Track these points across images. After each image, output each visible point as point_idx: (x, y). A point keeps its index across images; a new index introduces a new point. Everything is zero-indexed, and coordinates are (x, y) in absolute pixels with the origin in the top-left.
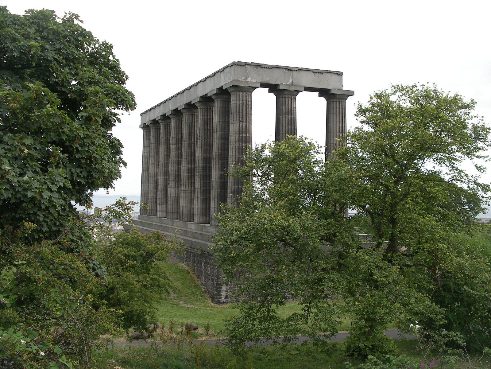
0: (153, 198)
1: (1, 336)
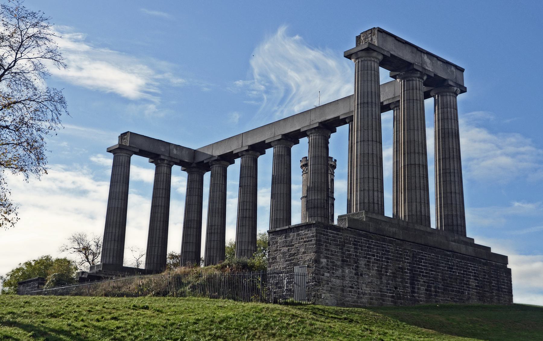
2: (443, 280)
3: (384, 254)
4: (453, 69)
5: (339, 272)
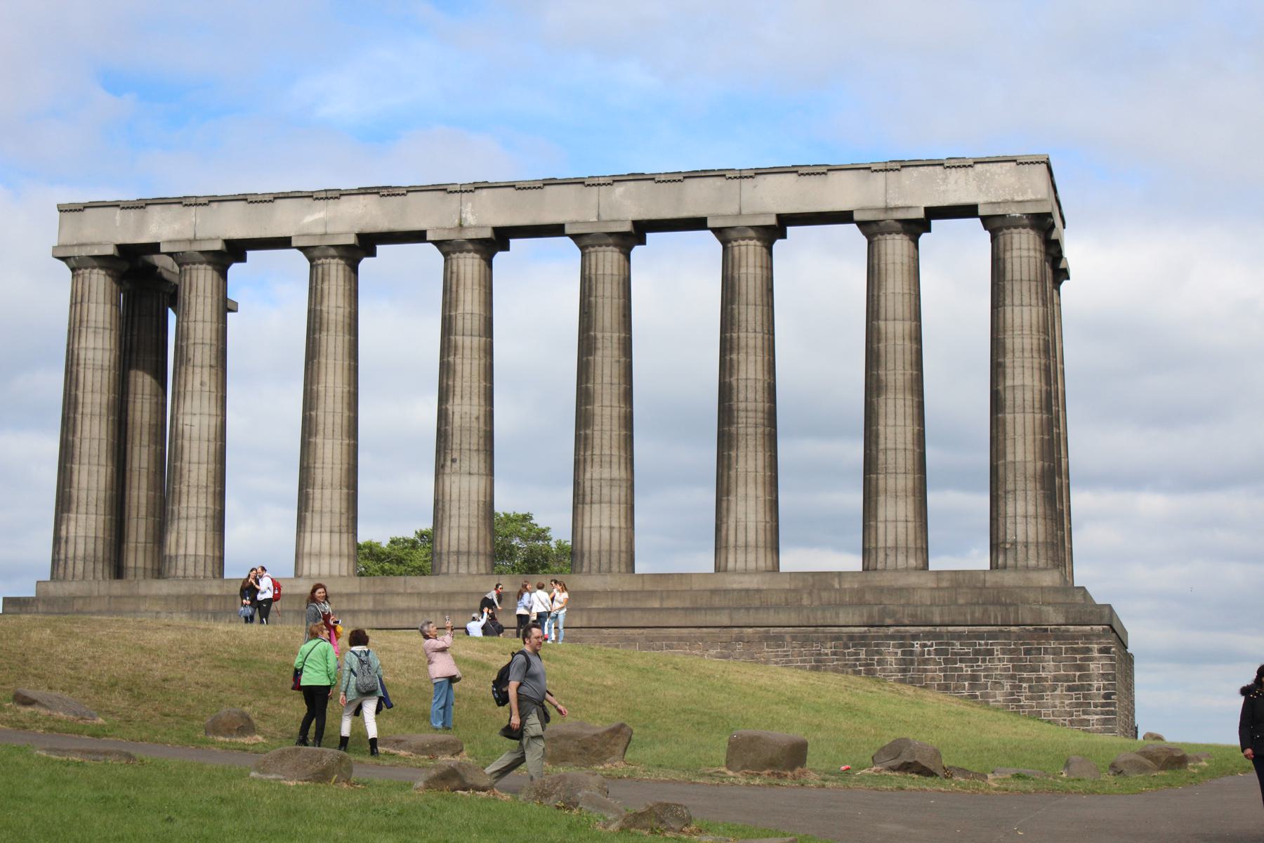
0: (210, 512)
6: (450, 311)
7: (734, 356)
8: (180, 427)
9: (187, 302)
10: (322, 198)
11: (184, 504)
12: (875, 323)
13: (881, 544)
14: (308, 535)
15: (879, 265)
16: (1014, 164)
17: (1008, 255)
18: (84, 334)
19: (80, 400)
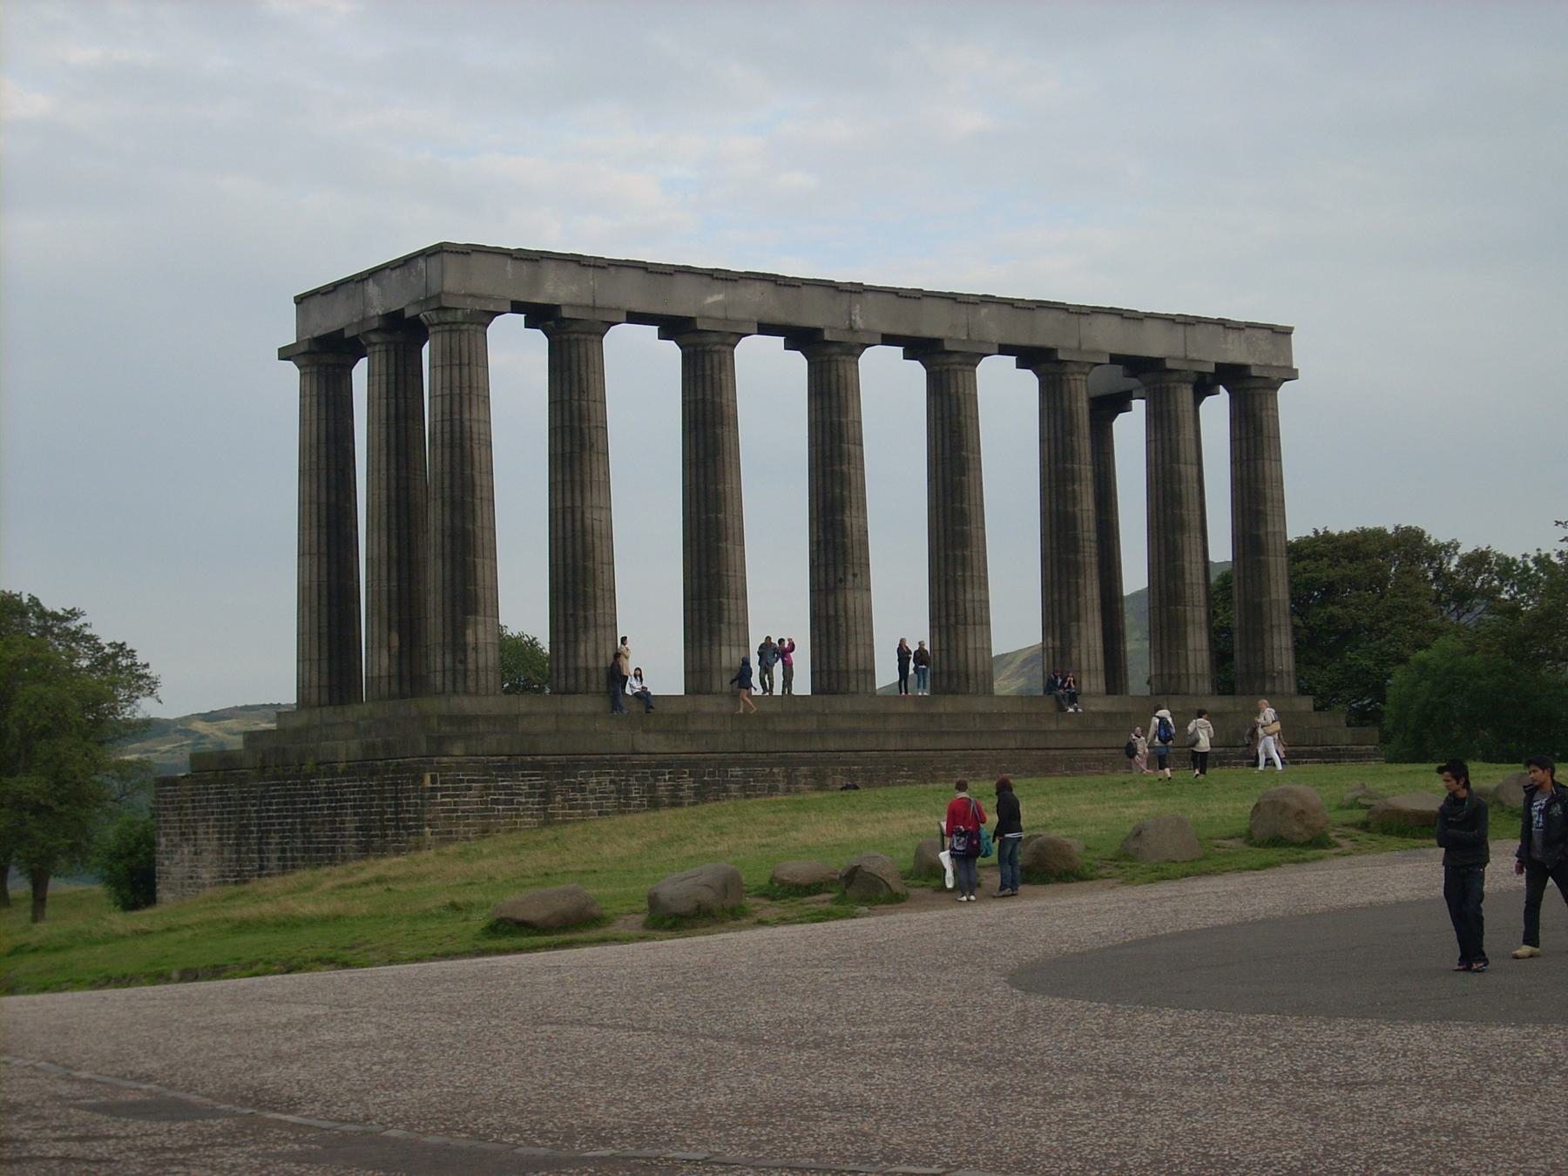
1: (1438, 1173)
2: (303, 830)
3: (224, 806)
4: (421, 263)
5: (177, 857)
6: (839, 417)
7: (1076, 487)
8: (588, 522)
9: (584, 377)
10: (722, 279)
11: (600, 611)
12: (1175, 466)
13: (1192, 670)
14: (725, 649)
15: (1176, 411)
16: (1270, 332)
17: (1264, 413)
18: (474, 402)
19: (478, 483)
